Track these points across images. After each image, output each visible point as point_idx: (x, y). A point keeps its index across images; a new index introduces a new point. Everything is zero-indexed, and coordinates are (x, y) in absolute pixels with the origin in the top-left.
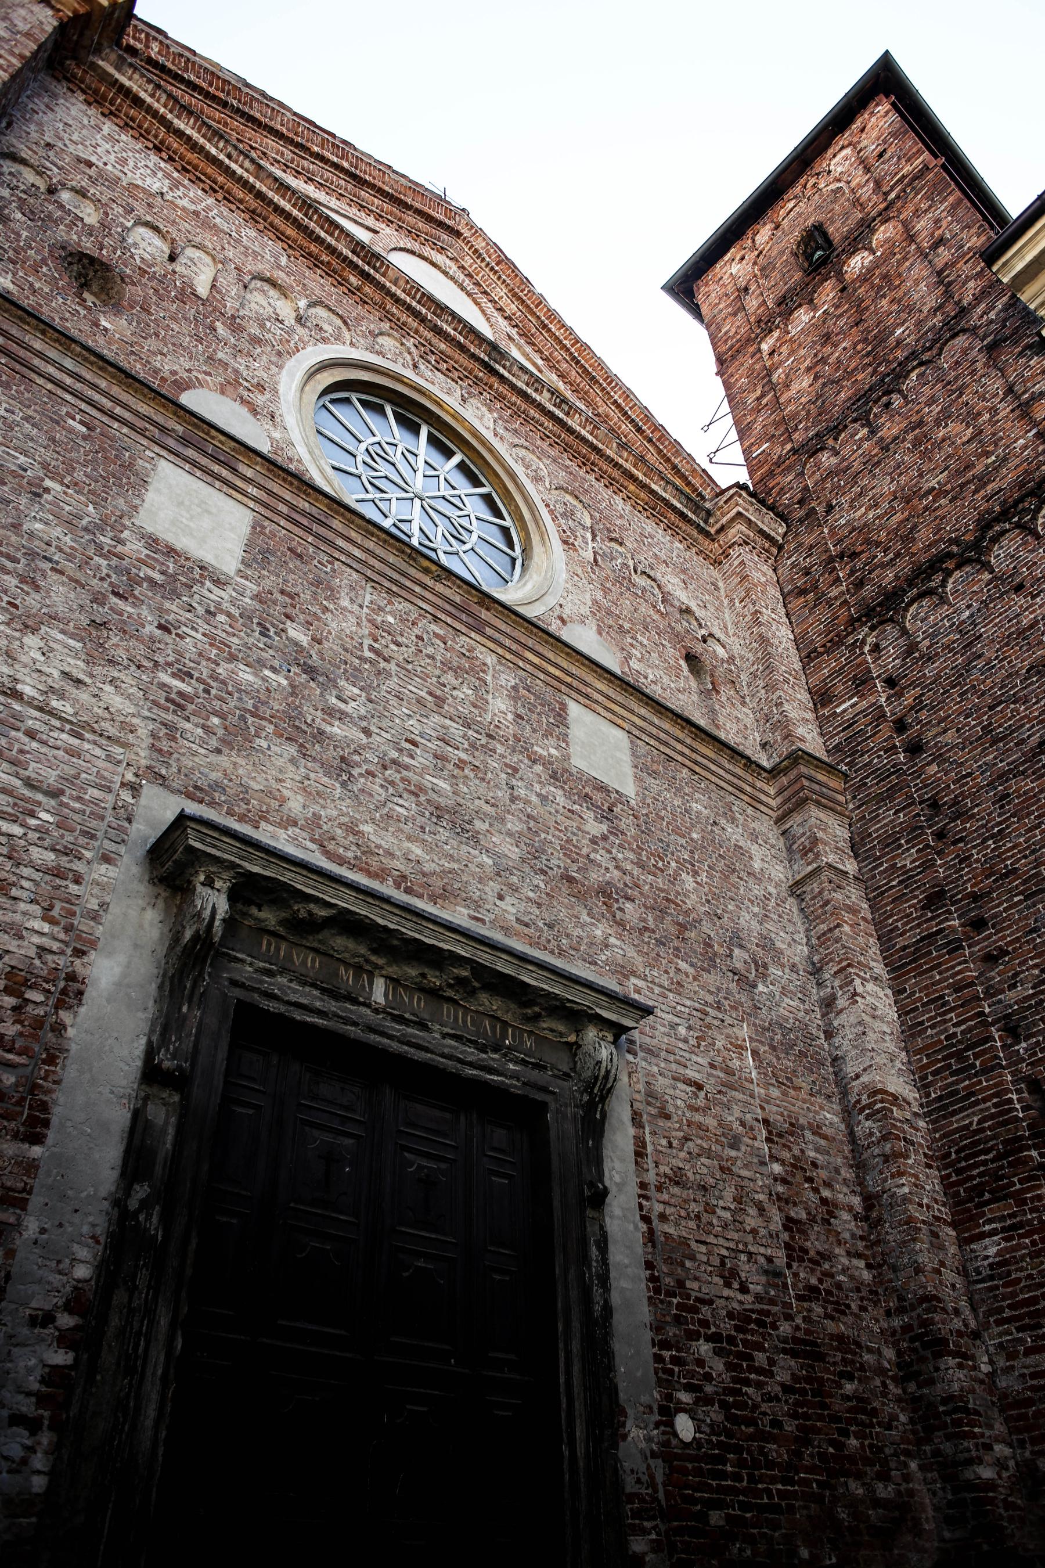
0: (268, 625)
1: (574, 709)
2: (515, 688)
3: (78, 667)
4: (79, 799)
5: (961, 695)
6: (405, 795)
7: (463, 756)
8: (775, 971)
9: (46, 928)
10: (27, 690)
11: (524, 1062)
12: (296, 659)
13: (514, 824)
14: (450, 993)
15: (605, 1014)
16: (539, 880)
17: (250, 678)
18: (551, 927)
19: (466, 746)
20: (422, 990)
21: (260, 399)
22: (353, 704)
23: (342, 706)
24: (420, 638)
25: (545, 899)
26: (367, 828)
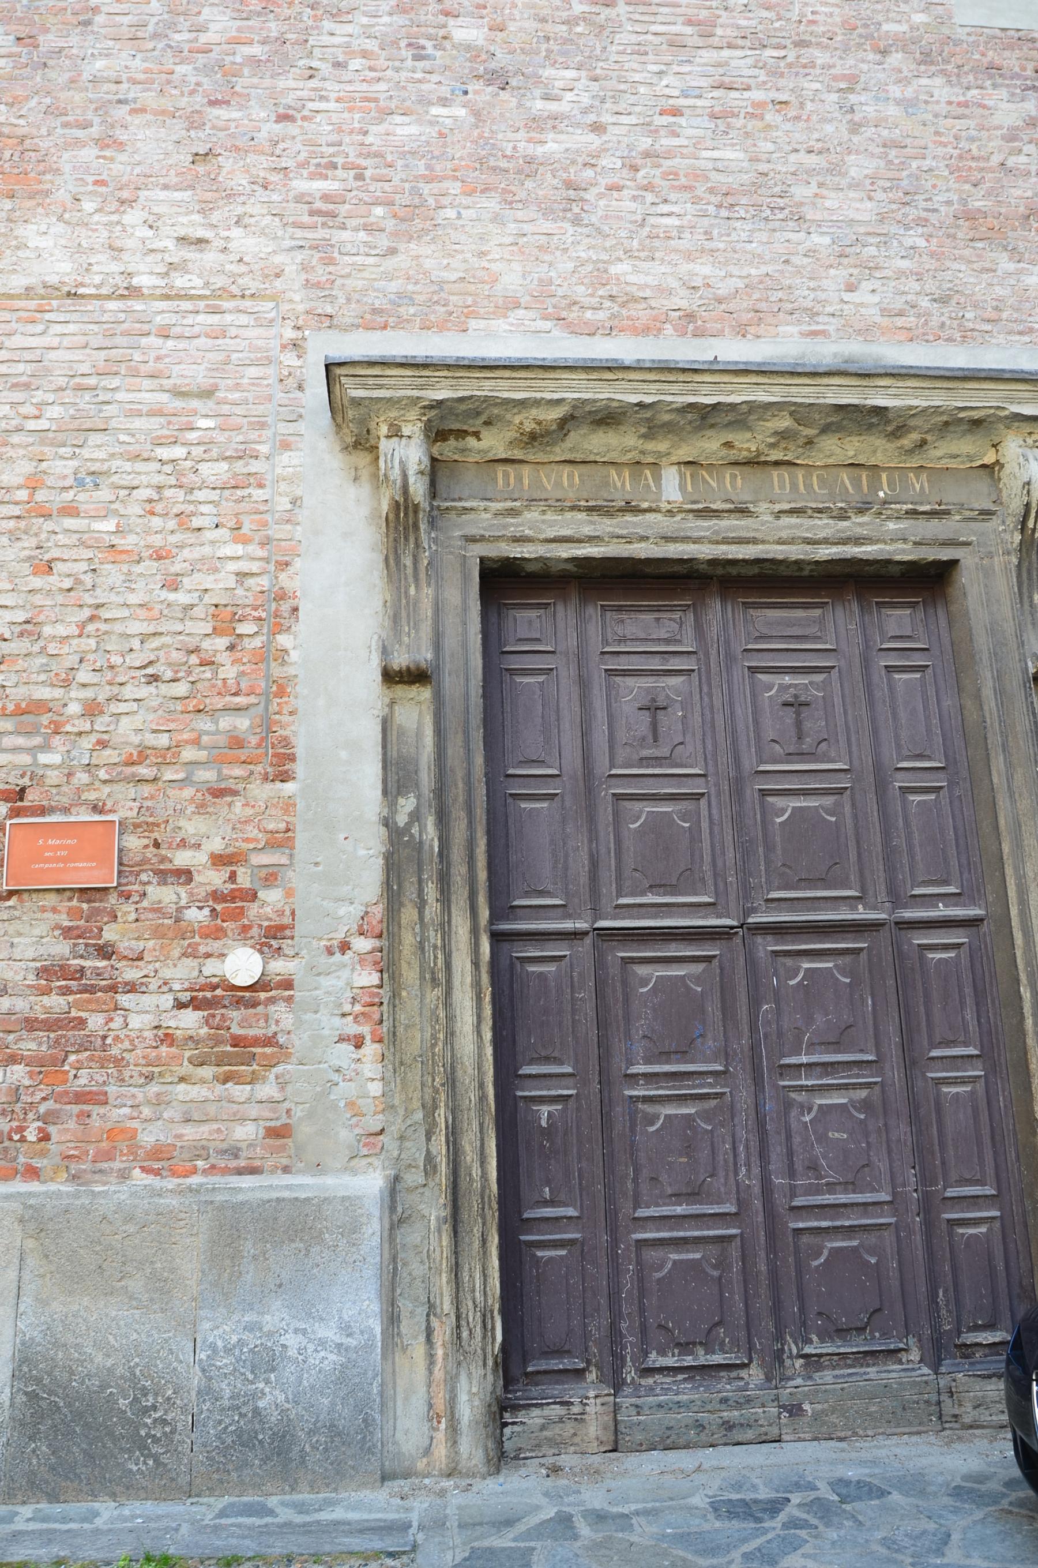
0: (422, 42)
4: (237, 387)
6: (673, 196)
7: (757, 95)
9: (239, 550)
10: (142, 281)
11: (913, 513)
12: (472, 69)
13: (859, 167)
14: (775, 455)
16: (915, 238)
17: (414, 129)
18: (943, 300)
19: (763, 78)
20: (736, 464)
22: (569, 96)
23: (553, 107)
25: (930, 264)
26: (615, 269)
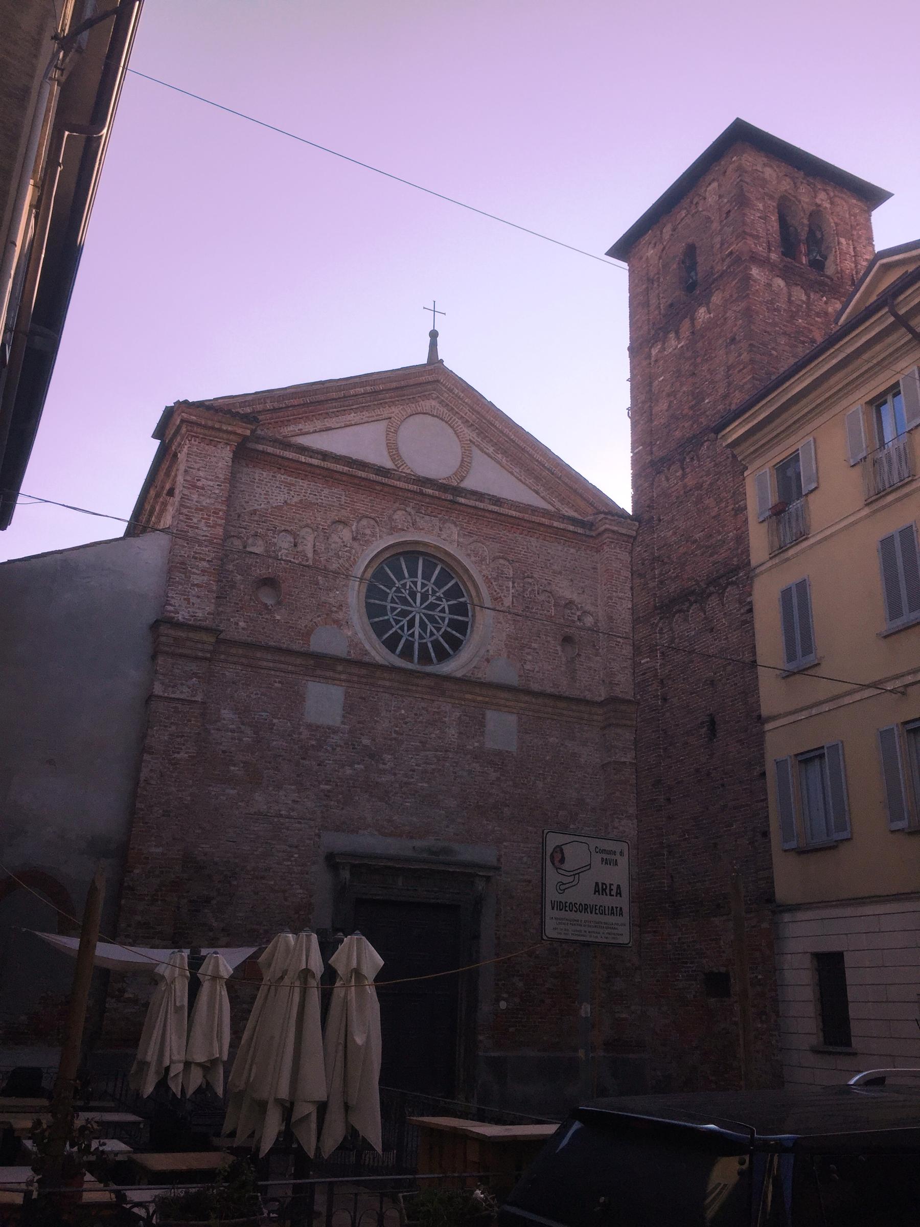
1: (489, 714)
2: (460, 718)
3: (295, 796)
5: (684, 679)
7: (433, 767)
9: (301, 891)
10: (283, 812)
15: (481, 874)
21: (340, 615)
24: (416, 714)
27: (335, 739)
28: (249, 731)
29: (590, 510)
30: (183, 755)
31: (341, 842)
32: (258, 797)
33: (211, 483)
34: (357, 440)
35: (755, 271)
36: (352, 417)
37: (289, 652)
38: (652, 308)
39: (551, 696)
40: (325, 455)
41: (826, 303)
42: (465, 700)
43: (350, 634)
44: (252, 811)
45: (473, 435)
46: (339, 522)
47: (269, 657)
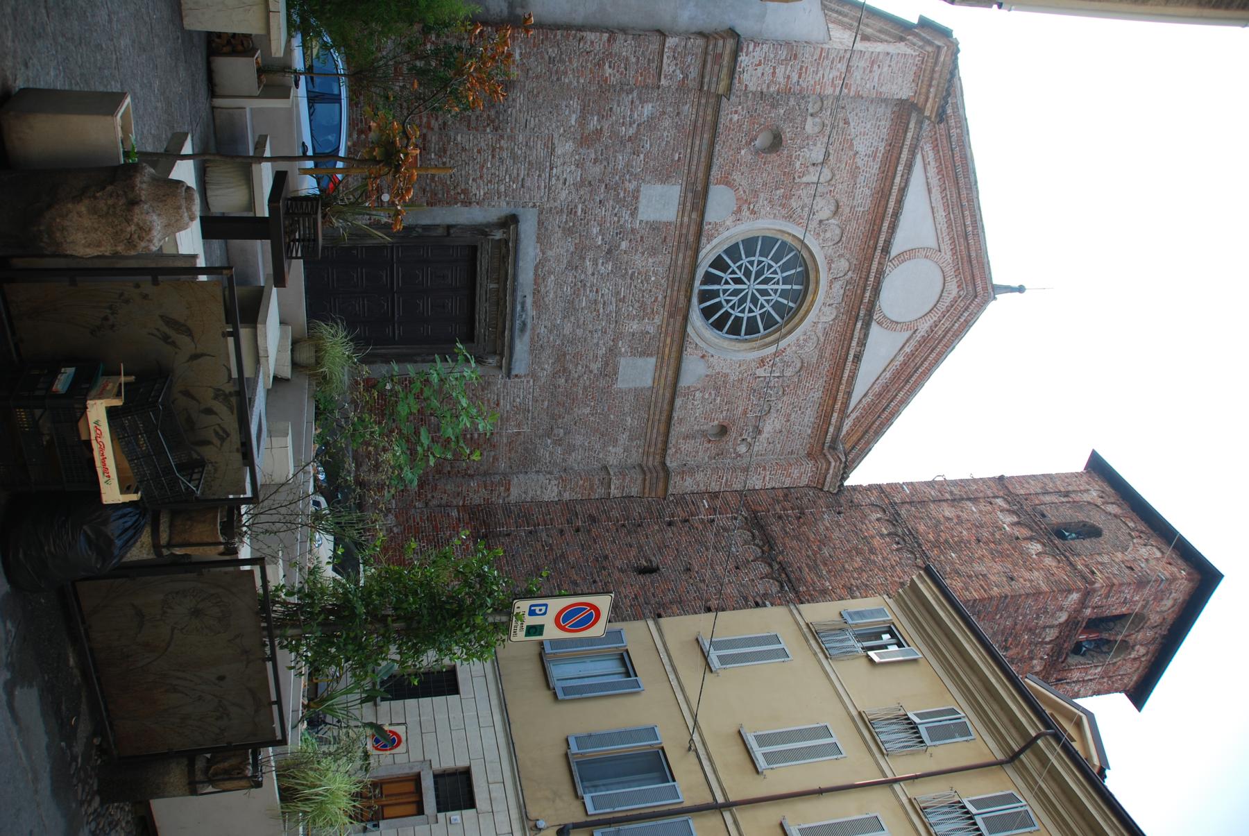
1: (652, 360)
2: (648, 333)
3: (570, 181)
8: (559, 450)
13: (579, 332)
21: (745, 213)
27: (626, 215)
28: (631, 131)
29: (847, 446)
30: (608, 71)
31: (528, 228)
32: (569, 146)
33: (876, 79)
34: (919, 220)
35: (1075, 596)
36: (941, 214)
37: (709, 167)
38: (1041, 497)
39: (670, 418)
40: (903, 190)
41: (1042, 658)
42: (666, 334)
43: (728, 223)
44: (556, 142)
45: (922, 331)
46: (838, 207)
47: (704, 147)
